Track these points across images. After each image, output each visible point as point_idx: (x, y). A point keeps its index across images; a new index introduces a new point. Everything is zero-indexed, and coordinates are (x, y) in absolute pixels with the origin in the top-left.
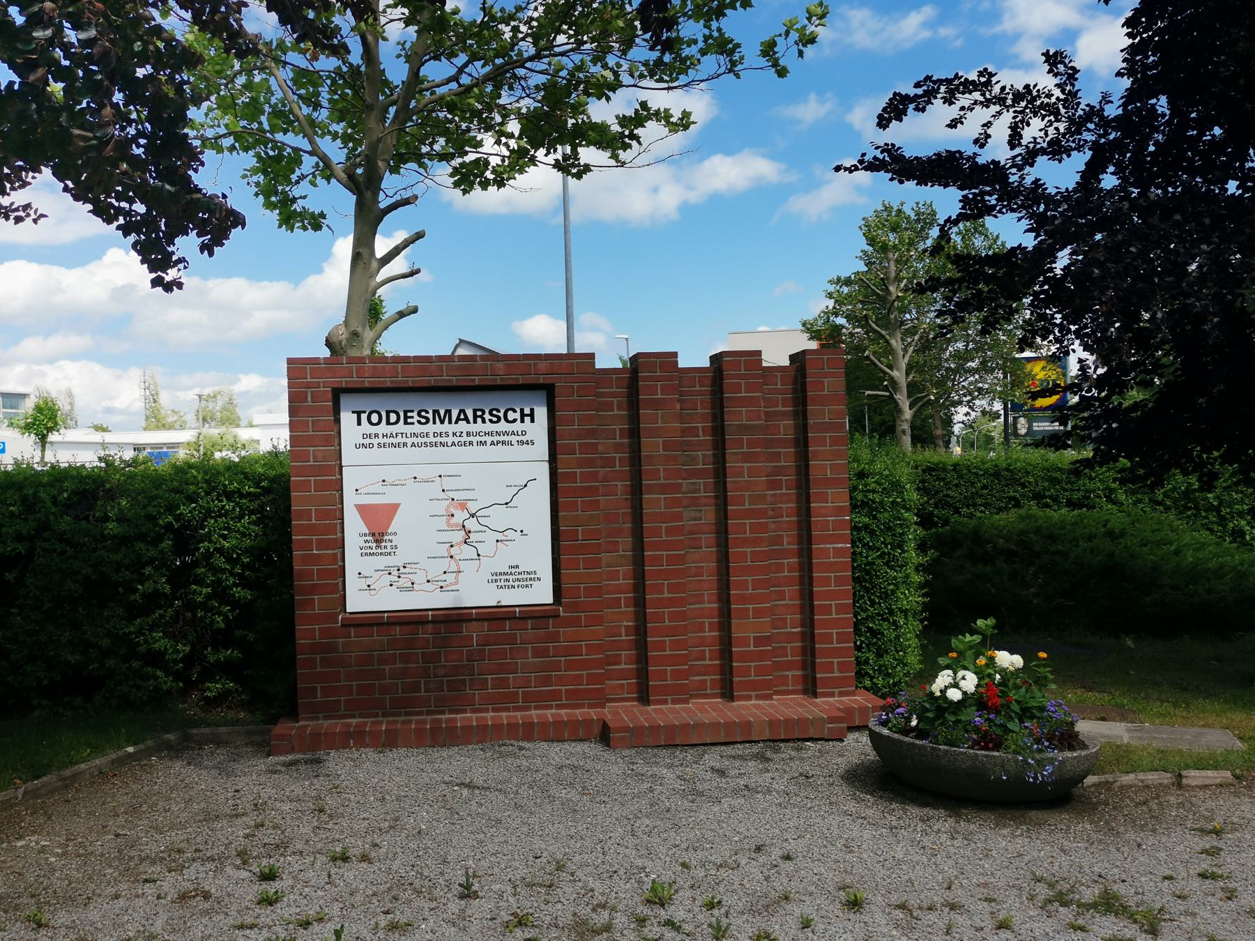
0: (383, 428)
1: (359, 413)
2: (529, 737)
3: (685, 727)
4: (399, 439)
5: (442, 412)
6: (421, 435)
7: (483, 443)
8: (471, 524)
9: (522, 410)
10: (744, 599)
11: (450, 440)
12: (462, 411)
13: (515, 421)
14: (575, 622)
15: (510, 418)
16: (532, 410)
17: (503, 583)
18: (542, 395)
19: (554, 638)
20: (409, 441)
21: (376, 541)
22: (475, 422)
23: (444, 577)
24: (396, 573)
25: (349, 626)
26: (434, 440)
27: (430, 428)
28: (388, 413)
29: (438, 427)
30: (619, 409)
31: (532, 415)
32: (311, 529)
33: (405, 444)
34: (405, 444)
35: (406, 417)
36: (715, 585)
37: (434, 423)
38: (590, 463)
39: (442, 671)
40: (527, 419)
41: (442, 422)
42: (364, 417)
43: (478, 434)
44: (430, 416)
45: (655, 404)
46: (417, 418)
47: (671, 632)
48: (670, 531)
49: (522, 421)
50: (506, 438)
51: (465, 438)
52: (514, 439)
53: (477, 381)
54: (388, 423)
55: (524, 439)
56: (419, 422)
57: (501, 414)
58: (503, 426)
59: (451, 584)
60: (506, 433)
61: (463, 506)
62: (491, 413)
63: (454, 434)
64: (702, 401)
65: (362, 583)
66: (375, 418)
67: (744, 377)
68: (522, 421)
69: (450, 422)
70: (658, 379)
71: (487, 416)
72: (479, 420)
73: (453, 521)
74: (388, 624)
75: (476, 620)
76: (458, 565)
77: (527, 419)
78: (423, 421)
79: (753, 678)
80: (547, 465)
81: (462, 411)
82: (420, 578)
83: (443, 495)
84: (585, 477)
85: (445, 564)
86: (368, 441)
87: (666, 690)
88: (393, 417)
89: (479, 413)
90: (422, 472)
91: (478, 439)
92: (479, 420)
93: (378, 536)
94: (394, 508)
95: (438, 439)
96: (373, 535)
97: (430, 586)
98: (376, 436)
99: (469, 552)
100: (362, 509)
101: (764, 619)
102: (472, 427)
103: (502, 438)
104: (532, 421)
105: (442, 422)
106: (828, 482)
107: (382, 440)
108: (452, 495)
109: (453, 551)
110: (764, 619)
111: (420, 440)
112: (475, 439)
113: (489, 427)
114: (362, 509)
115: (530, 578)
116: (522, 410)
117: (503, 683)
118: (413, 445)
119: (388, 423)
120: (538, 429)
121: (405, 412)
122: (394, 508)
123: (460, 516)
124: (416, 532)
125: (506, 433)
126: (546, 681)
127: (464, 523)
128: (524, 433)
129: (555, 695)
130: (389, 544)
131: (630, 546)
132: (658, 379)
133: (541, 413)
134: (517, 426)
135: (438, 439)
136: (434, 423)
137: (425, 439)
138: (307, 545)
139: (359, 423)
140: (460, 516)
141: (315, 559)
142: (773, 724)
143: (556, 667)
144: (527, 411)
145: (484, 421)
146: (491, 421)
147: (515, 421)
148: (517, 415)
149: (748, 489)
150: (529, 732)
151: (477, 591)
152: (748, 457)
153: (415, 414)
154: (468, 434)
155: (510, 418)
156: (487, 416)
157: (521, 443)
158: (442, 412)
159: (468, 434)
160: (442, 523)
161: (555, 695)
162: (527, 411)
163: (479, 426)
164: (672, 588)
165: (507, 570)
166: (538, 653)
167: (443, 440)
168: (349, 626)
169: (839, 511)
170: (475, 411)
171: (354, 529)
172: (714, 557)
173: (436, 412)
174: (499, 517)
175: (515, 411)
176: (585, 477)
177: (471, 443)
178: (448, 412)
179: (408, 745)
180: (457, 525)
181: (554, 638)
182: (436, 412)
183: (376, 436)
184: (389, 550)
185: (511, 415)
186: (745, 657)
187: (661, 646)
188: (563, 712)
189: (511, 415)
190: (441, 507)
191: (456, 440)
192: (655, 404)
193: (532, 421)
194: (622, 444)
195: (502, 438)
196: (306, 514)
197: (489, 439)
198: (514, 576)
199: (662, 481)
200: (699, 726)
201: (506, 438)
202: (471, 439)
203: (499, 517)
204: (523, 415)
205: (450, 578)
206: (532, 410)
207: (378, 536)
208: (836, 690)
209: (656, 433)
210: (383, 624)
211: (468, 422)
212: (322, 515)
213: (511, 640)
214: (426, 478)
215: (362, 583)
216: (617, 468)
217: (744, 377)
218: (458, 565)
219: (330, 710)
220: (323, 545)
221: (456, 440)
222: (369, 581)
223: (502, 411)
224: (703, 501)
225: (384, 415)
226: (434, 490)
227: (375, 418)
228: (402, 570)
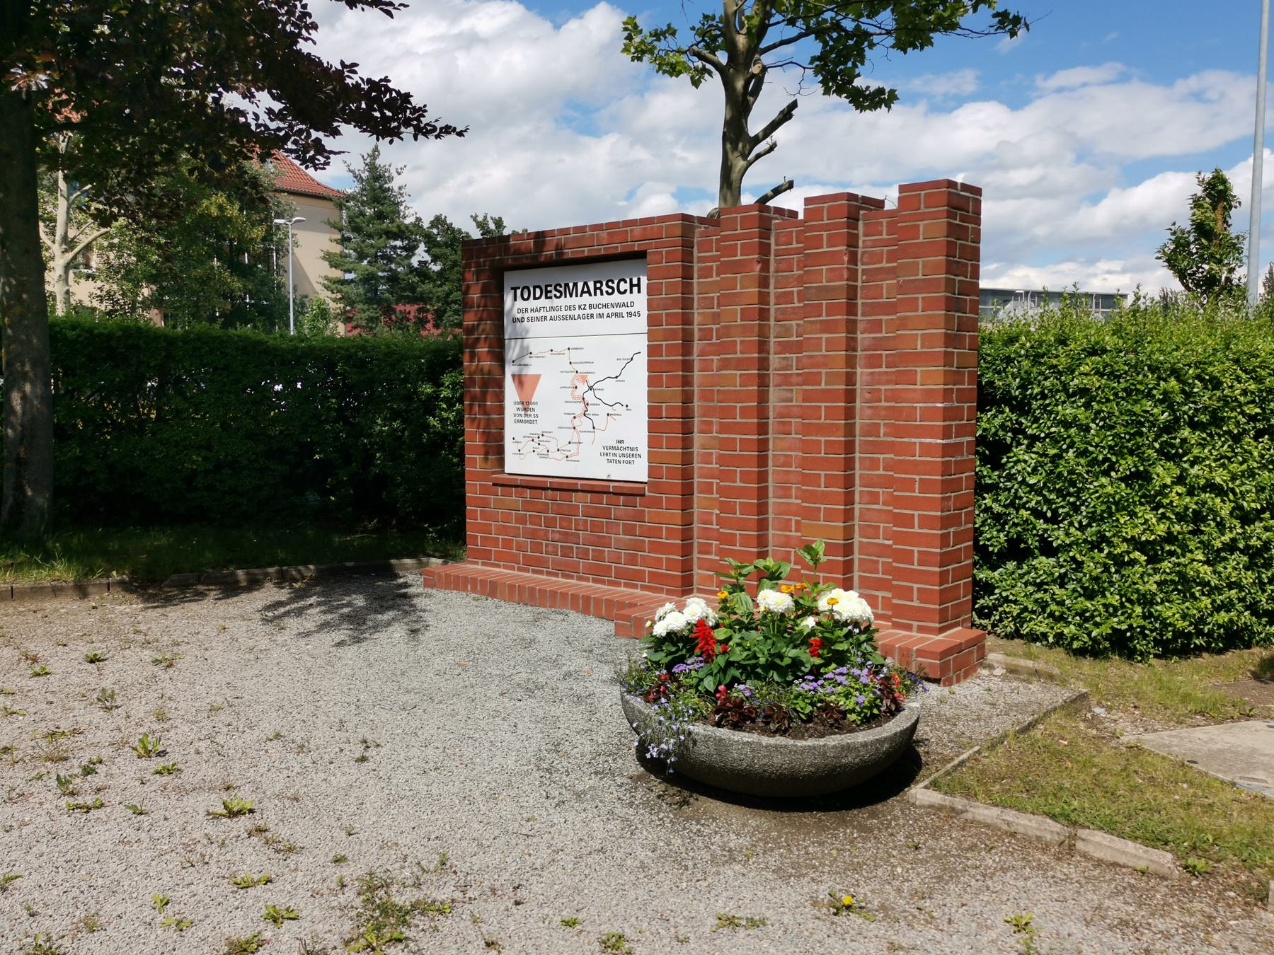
1: (515, 289)
4: (542, 314)
5: (571, 285)
7: (600, 316)
8: (589, 397)
11: (577, 313)
12: (586, 284)
17: (611, 458)
20: (548, 315)
28: (535, 288)
31: (638, 285)
35: (547, 292)
39: (557, 536)
42: (519, 292)
50: (618, 310)
51: (588, 311)
52: (624, 310)
57: (615, 286)
58: (616, 297)
60: (618, 305)
67: (826, 228)
71: (604, 288)
81: (586, 284)
83: (570, 368)
85: (569, 435)
91: (598, 311)
95: (568, 313)
99: (585, 424)
108: (577, 367)
109: (576, 422)
113: (606, 299)
115: (633, 454)
117: (599, 556)
119: (535, 298)
125: (618, 305)
126: (632, 560)
129: (638, 576)
134: (627, 298)
135: (568, 313)
140: (583, 388)
144: (635, 282)
149: (825, 366)
151: (591, 465)
156: (604, 288)
157: (630, 314)
158: (571, 285)
161: (638, 576)
162: (635, 282)
166: (629, 531)
167: (571, 313)
169: (929, 395)
170: (595, 283)
181: (640, 517)
189: (624, 286)
190: (568, 379)
191: (581, 312)
197: (605, 311)
198: (618, 452)
199: (739, 355)
201: (618, 310)
202: (593, 311)
203: (610, 392)
204: (632, 286)
207: (526, 405)
208: (915, 624)
219: (484, 556)
221: (581, 312)
224: (794, 379)
226: (564, 360)
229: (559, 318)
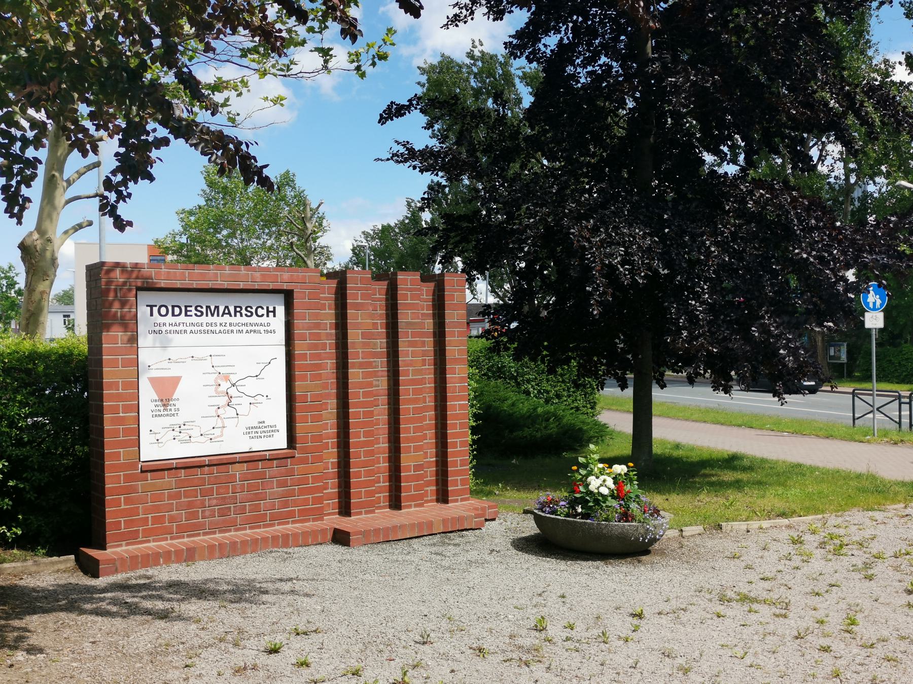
0: (169, 319)
1: (151, 307)
2: (286, 545)
3: (395, 528)
4: (181, 328)
5: (213, 308)
6: (197, 325)
7: (240, 332)
8: (233, 391)
9: (268, 308)
10: (409, 440)
11: (218, 329)
12: (227, 307)
13: (263, 315)
14: (304, 461)
15: (260, 314)
16: (274, 308)
17: (253, 435)
18: (281, 298)
19: (291, 473)
20: (189, 329)
21: (164, 405)
22: (235, 315)
23: (213, 431)
24: (178, 429)
25: (146, 471)
26: (207, 328)
27: (204, 319)
28: (173, 307)
29: (210, 319)
30: (330, 309)
31: (274, 312)
32: (119, 397)
33: (185, 331)
34: (185, 331)
35: (186, 311)
36: (387, 432)
37: (207, 315)
38: (315, 347)
39: (215, 502)
40: (271, 314)
41: (212, 315)
42: (155, 309)
43: (237, 324)
44: (204, 310)
45: (358, 307)
46: (194, 312)
47: (364, 464)
48: (366, 395)
49: (268, 316)
50: (256, 328)
51: (228, 328)
52: (262, 329)
53: (242, 286)
54: (173, 315)
55: (269, 329)
56: (196, 315)
57: (253, 311)
58: (254, 319)
59: (218, 437)
60: (256, 325)
61: (226, 378)
62: (246, 310)
63: (221, 324)
64: (381, 305)
65: (153, 438)
66: (163, 311)
67: (410, 290)
68: (268, 316)
69: (218, 315)
70: (359, 289)
71: (244, 312)
72: (238, 314)
73: (220, 389)
74: (176, 468)
75: (239, 462)
76: (223, 422)
77: (271, 314)
78: (199, 314)
79: (413, 493)
80: (284, 348)
81: (227, 307)
82: (195, 433)
83: (213, 370)
84: (313, 356)
85: (213, 421)
86: (157, 328)
87: (361, 505)
88: (177, 311)
89: (238, 309)
90: (198, 352)
91: (237, 328)
92: (238, 314)
93: (165, 401)
94: (176, 381)
95: (210, 328)
96: (162, 400)
97: (202, 439)
98: (164, 324)
99: (231, 412)
100: (153, 381)
101: (418, 455)
102: (233, 320)
103: (253, 328)
104: (274, 316)
105: (212, 315)
106: (456, 361)
107: (168, 328)
108: (219, 370)
109: (220, 412)
110: (418, 455)
111: (196, 328)
112: (235, 329)
113: (245, 320)
114: (153, 381)
115: (274, 430)
116: (268, 308)
117: (257, 508)
118: (191, 332)
119: (173, 315)
120: (278, 322)
121: (186, 307)
122: (176, 381)
123: (225, 385)
124: (194, 397)
125: (256, 325)
126: (285, 505)
127: (227, 391)
128: (269, 324)
129: (291, 514)
130: (173, 408)
131: (335, 406)
132: (359, 289)
133: (281, 310)
134: (264, 320)
135: (210, 328)
136: (207, 315)
137: (200, 328)
138: (115, 410)
139: (152, 315)
140: (225, 385)
141: (121, 421)
142: (445, 521)
143: (291, 494)
144: (271, 309)
145: (241, 315)
146: (246, 315)
147: (263, 315)
148: (264, 312)
149: (411, 365)
150: (285, 541)
151: (236, 442)
152: (412, 344)
153: (193, 309)
154: (230, 325)
155: (260, 314)
156: (244, 312)
157: (267, 332)
158: (213, 308)
159: (230, 325)
160: (212, 390)
161: (291, 514)
162: (271, 309)
163: (238, 319)
164: (367, 434)
165: (256, 425)
166: (282, 484)
167: (213, 328)
168: (146, 471)
169: (462, 380)
170: (235, 307)
171: (147, 395)
172: (386, 412)
173: (208, 307)
174: (251, 386)
175: (263, 308)
176: (313, 356)
177: (232, 331)
178: (217, 307)
179: (203, 559)
180: (222, 392)
181: (291, 473)
182: (208, 307)
183: (164, 324)
184: (173, 412)
185: (260, 312)
186: (409, 479)
187: (358, 475)
188: (297, 525)
189: (260, 312)
190: (211, 379)
191: (222, 328)
192: (358, 307)
193: (274, 316)
194: (331, 334)
195: (253, 328)
196: (115, 385)
197: (245, 329)
198: (261, 429)
199: (361, 360)
200: (403, 527)
201: (256, 328)
202: (232, 328)
203: (251, 386)
204: (268, 312)
205: (217, 432)
206: (274, 308)
207: (165, 401)
209: (357, 326)
210: (172, 469)
211: (231, 316)
212: (126, 386)
213: (262, 476)
214: (200, 357)
215: (153, 438)
216: (328, 351)
217: (410, 290)
218: (223, 422)
219: (131, 537)
220: (127, 409)
221: (222, 328)
222: (158, 437)
223: (254, 308)
224: (380, 374)
225: (170, 308)
226: (206, 366)
227: (163, 311)
228: (183, 427)
229: (225, 332)
